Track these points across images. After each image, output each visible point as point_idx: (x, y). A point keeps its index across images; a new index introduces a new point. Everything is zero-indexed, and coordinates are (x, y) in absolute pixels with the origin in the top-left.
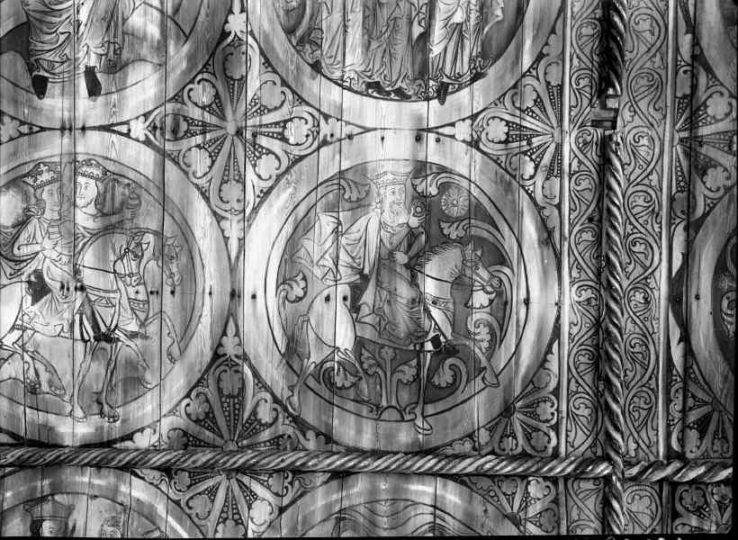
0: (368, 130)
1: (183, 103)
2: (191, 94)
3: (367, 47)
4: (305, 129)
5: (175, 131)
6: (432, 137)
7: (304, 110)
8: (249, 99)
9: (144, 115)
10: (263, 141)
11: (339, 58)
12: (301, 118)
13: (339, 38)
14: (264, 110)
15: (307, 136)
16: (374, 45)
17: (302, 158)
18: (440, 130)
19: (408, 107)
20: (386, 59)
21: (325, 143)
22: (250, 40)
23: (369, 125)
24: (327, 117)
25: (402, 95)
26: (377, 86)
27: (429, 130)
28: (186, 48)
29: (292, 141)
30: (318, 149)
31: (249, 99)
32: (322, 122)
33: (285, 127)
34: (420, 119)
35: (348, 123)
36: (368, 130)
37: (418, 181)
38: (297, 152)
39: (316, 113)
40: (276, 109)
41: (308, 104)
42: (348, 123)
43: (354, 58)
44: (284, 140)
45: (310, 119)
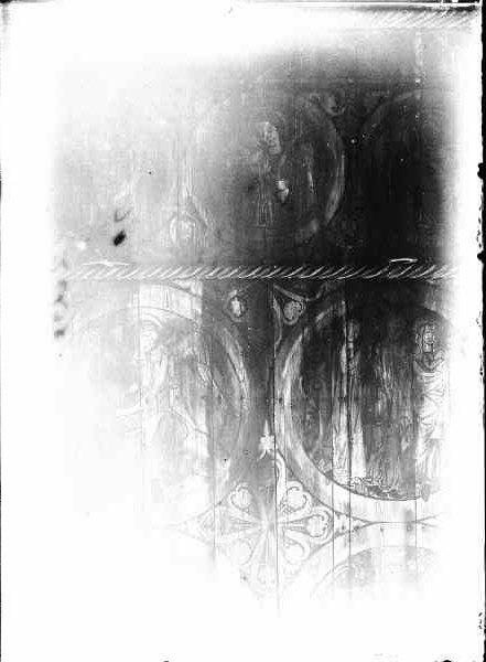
0: (371, 524)
1: (228, 507)
2: (234, 500)
3: (367, 460)
4: (322, 524)
5: (222, 528)
6: (419, 526)
7: (321, 509)
8: (278, 503)
9: (199, 517)
10: (289, 534)
11: (346, 468)
12: (318, 516)
13: (346, 454)
14: (292, 510)
15: (324, 529)
16: (373, 457)
17: (320, 547)
18: (425, 522)
19: (402, 504)
20: (383, 468)
21: (338, 534)
22: (278, 456)
23: (371, 518)
24: (339, 514)
25: (396, 496)
26: (377, 490)
27: (416, 522)
28: (228, 464)
29: (313, 534)
30: (333, 538)
31: (278, 503)
32: (336, 517)
33: (307, 523)
34: (408, 513)
35: (355, 519)
36: (371, 524)
37: (409, 563)
38: (317, 541)
39: (331, 512)
40: (299, 509)
41: (323, 504)
42: (355, 519)
43: (359, 470)
44: (306, 533)
45: (326, 516)
